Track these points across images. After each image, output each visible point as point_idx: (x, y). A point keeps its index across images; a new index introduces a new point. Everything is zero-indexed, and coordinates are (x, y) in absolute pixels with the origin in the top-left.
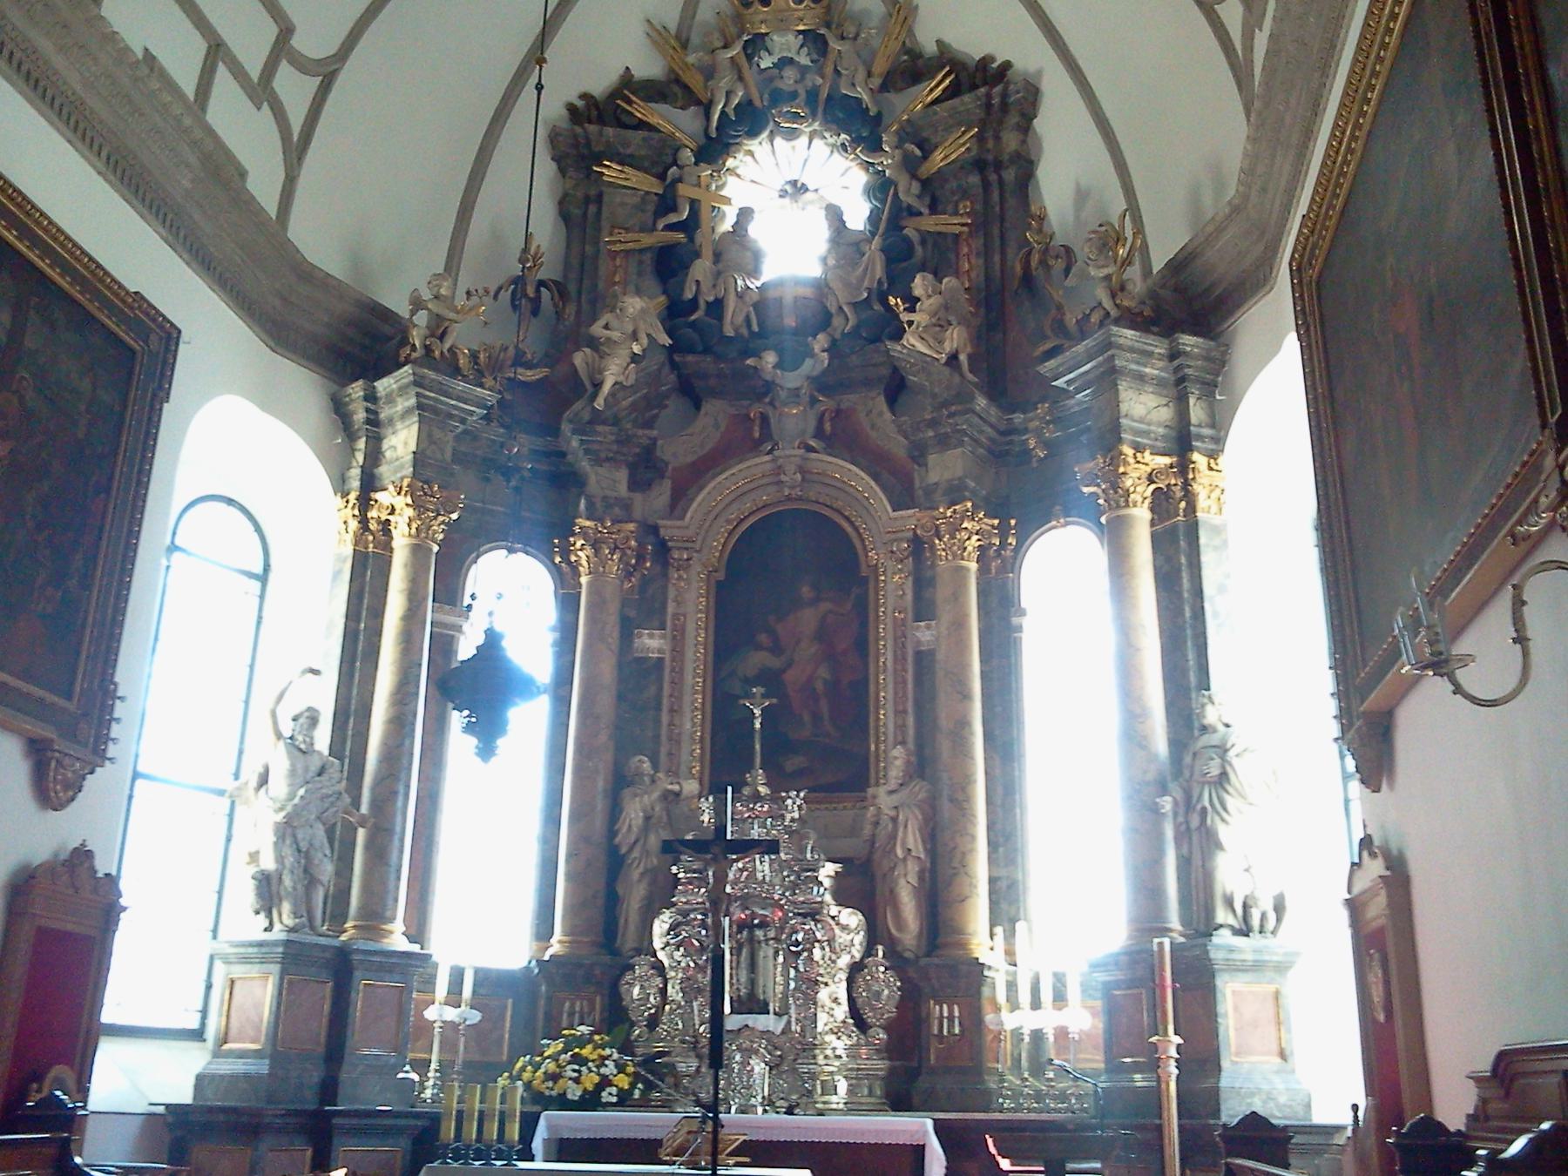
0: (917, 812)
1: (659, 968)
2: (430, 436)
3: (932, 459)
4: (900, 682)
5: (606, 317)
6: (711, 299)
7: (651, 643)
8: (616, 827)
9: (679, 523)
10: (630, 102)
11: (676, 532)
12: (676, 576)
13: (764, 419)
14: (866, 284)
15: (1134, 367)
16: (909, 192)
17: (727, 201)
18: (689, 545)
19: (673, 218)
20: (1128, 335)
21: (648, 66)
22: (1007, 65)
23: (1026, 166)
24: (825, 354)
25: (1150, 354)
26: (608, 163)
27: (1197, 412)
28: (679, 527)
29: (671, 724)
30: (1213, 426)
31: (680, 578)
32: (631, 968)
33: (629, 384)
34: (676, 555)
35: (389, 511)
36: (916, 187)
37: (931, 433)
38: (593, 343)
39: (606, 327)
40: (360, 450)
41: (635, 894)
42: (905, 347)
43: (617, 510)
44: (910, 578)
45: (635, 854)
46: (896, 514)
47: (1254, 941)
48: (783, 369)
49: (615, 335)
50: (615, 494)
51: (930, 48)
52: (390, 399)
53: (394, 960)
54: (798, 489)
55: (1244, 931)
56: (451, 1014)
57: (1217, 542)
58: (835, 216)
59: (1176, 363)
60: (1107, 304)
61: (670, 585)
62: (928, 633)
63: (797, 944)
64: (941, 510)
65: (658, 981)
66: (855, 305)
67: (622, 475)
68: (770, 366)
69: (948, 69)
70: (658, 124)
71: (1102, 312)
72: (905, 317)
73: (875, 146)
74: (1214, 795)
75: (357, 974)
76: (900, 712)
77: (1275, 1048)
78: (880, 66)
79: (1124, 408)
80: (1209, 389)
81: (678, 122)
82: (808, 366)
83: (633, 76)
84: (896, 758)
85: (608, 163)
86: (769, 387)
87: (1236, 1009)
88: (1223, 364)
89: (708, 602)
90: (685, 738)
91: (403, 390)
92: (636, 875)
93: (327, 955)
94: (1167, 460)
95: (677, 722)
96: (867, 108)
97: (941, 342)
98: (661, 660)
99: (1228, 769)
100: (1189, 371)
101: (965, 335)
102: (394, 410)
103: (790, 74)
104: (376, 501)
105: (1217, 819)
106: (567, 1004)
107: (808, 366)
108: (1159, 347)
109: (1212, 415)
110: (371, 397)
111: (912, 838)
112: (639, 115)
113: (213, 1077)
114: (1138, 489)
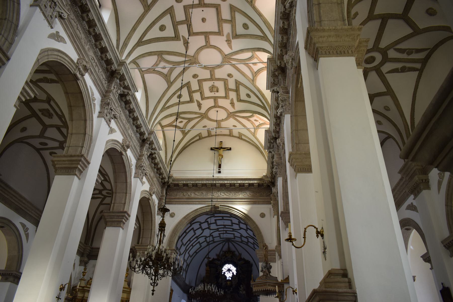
19: (217, 273)
21: (216, 257)
22: (250, 261)
51: (242, 257)
58: (233, 273)
78: (238, 259)
107: (230, 291)
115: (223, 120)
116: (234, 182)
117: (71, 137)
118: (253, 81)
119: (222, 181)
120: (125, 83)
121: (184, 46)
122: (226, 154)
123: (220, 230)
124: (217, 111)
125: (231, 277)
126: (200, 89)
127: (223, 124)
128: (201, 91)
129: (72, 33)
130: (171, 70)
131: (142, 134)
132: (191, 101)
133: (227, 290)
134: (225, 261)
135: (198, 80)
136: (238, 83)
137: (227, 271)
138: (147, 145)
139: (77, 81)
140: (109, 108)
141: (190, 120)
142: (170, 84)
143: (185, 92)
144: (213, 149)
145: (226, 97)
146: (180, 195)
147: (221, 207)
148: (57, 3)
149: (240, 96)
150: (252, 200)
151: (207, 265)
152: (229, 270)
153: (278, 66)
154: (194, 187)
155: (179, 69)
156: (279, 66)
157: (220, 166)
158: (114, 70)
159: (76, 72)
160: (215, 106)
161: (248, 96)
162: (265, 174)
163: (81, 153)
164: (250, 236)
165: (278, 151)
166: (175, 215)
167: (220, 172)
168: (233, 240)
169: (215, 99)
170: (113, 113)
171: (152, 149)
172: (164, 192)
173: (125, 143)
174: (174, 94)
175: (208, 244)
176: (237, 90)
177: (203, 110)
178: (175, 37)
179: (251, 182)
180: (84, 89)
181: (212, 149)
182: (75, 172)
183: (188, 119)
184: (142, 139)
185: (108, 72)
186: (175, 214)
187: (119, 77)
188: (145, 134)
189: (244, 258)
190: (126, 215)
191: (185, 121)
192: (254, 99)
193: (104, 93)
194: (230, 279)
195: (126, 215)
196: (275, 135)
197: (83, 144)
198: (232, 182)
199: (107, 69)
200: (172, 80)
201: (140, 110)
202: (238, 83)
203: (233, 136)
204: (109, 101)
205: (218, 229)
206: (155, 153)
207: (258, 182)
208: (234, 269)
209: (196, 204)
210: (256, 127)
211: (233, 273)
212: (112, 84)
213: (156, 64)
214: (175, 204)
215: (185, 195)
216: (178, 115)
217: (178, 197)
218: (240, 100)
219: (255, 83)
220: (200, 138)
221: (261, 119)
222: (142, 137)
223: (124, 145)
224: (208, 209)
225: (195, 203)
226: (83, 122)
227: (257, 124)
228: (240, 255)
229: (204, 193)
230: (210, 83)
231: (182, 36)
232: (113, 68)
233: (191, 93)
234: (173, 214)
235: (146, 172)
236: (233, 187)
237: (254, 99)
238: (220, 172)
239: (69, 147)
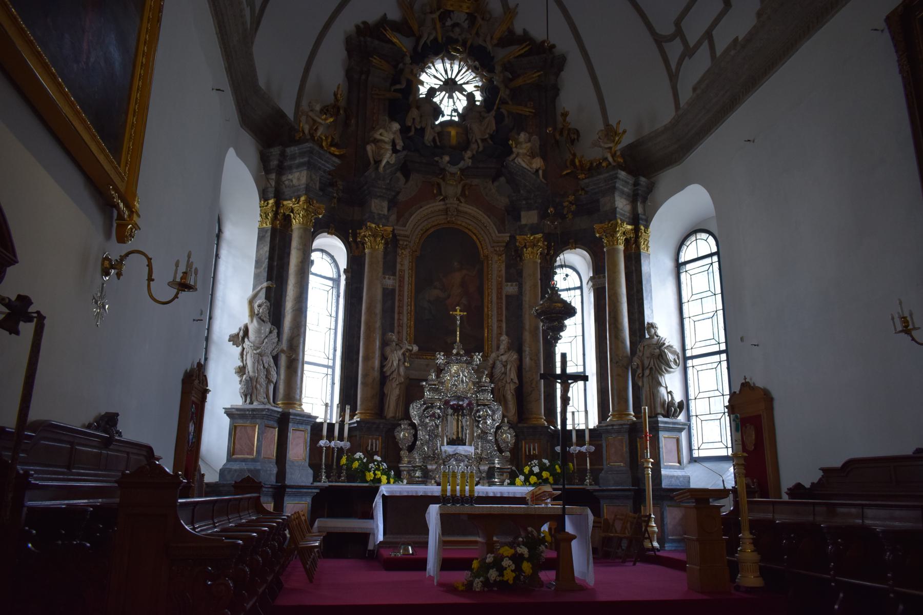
0: (514, 363)
1: (413, 426)
2: (311, 177)
3: (523, 214)
4: (499, 308)
5: (381, 131)
6: (419, 127)
7: (511, 289)
8: (385, 363)
9: (404, 228)
10: (386, 30)
11: (402, 233)
12: (400, 252)
13: (439, 185)
14: (488, 131)
15: (621, 187)
16: (504, 93)
17: (422, 83)
18: (406, 239)
19: (398, 87)
20: (622, 174)
21: (394, 14)
22: (553, 46)
23: (556, 90)
24: (470, 160)
25: (627, 183)
26: (375, 56)
27: (640, 210)
28: (403, 230)
29: (399, 319)
30: (644, 214)
31: (402, 253)
32: (400, 425)
33: (392, 163)
34: (401, 242)
35: (290, 211)
36: (508, 92)
37: (524, 202)
38: (376, 141)
39: (381, 135)
40: (272, 179)
41: (394, 393)
42: (516, 163)
43: (384, 220)
44: (504, 263)
45: (395, 375)
46: (500, 235)
48: (451, 164)
49: (386, 139)
50: (383, 213)
52: (293, 157)
53: (305, 419)
54: (454, 219)
55: (667, 415)
56: (341, 444)
57: (647, 262)
58: (470, 97)
59: (636, 188)
60: (610, 159)
61: (398, 256)
62: (512, 288)
63: (479, 417)
64: (528, 236)
65: (412, 431)
66: (483, 140)
67: (385, 204)
68: (446, 162)
69: (528, 43)
70: (396, 42)
71: (607, 162)
72: (514, 150)
73: (491, 70)
74: (655, 361)
75: (290, 425)
76: (499, 321)
77: (677, 460)
79: (617, 203)
80: (644, 201)
81: (403, 43)
82: (462, 165)
83: (387, 18)
84: (503, 340)
85: (375, 56)
86: (443, 170)
87: (665, 445)
88: (651, 191)
89: (412, 265)
90: (405, 326)
91: (302, 154)
92: (394, 385)
93: (279, 416)
94: (629, 227)
95: (401, 318)
96: (489, 52)
97: (531, 164)
99: (663, 354)
100: (640, 192)
101: (542, 162)
102: (292, 162)
103: (457, 30)
104: (283, 205)
105: (657, 372)
106: (370, 441)
107: (462, 165)
108: (631, 180)
109: (644, 210)
110: (283, 155)
111: (513, 375)
112: (388, 36)
113: (230, 470)
114: (621, 238)
125: (459, 115)
133: (447, 158)
134: (436, 39)
137: (441, 89)
152: (450, 86)
189: (525, 32)
194: (456, 119)
208: (471, 82)
211: (470, 97)
228: (510, 12)
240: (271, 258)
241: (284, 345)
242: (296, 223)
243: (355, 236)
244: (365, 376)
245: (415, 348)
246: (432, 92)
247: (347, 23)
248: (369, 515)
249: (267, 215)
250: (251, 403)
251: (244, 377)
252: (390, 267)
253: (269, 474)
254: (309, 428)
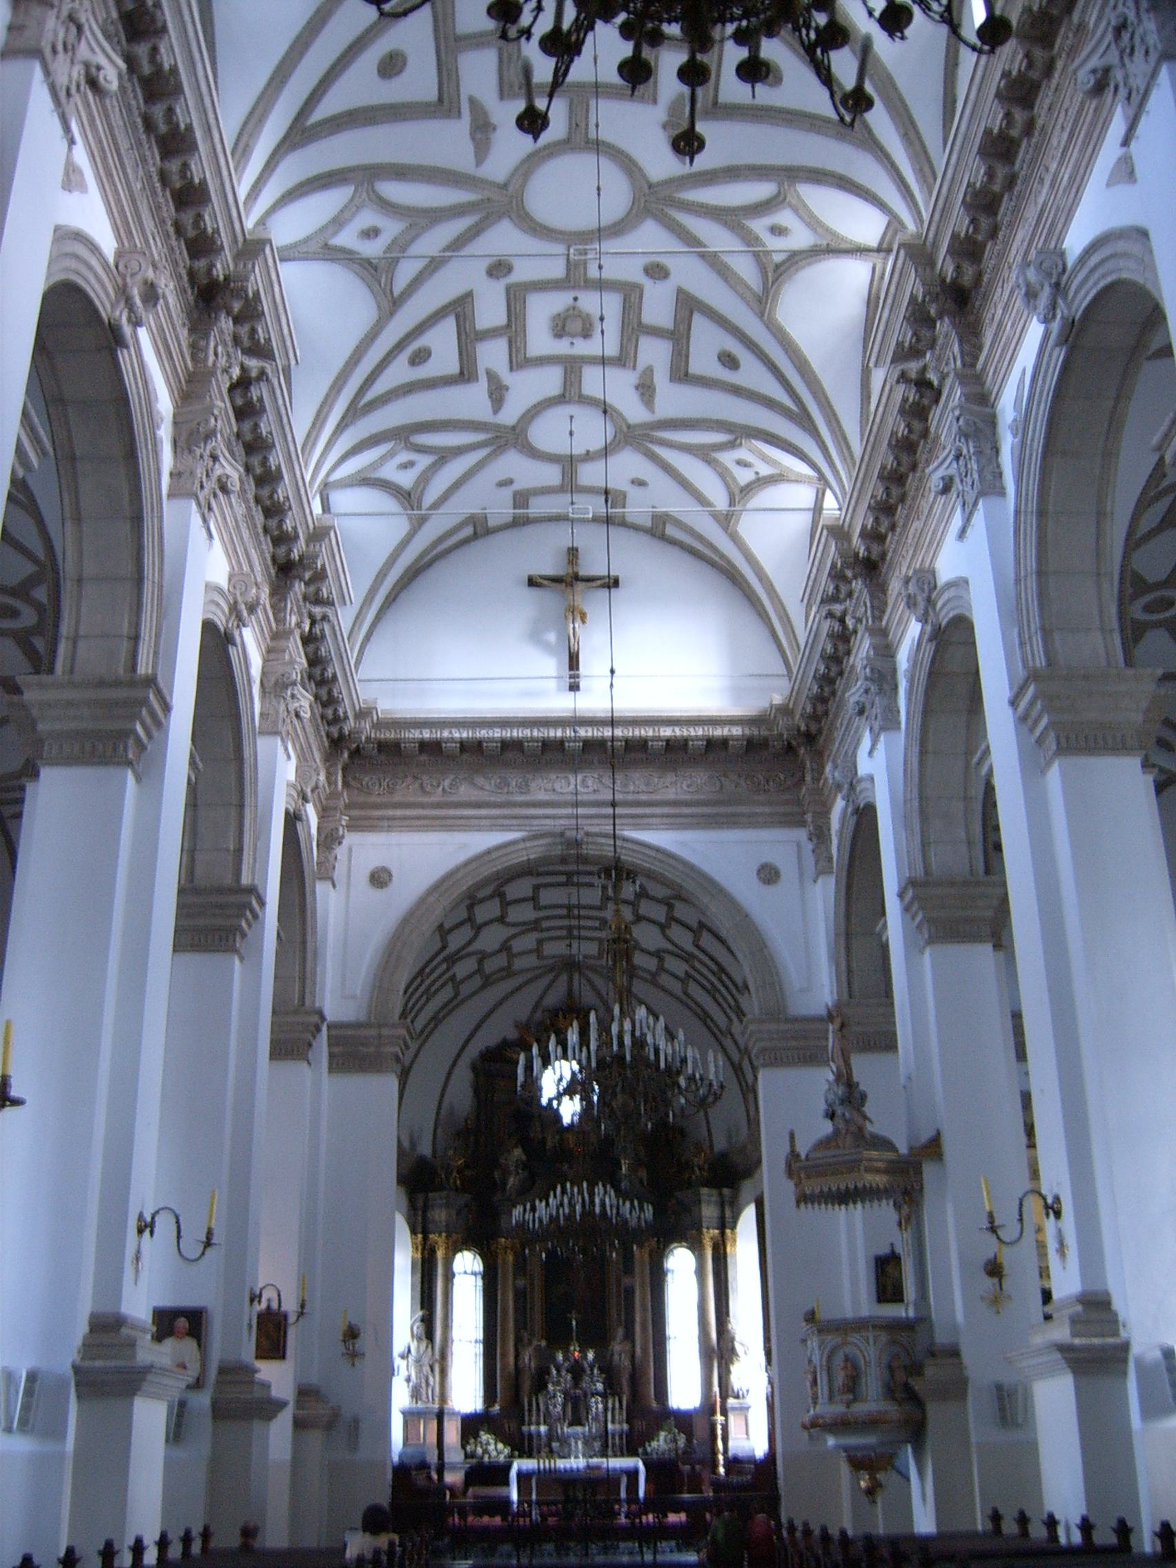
21: (512, 1034)
27: (728, 1213)
41: (527, 1385)
47: (741, 1401)
79: (703, 1213)
94: (717, 1231)
98: (525, 1288)
108: (714, 1192)
115: (588, 457)
116: (643, 732)
117: (80, 592)
118: (763, 302)
119: (590, 729)
120: (260, 331)
121: (473, 139)
122: (594, 602)
123: (545, 924)
124: (572, 417)
126: (509, 326)
127: (590, 474)
128: (514, 329)
129: (100, 142)
130: (399, 247)
131: (281, 539)
132: (465, 375)
135: (508, 289)
136: (688, 305)
138: (299, 588)
139: (116, 350)
140: (208, 452)
141: (444, 456)
142: (392, 304)
143: (443, 340)
144: (539, 580)
145: (623, 359)
146: (406, 790)
147: (590, 839)
148: (86, 28)
149: (687, 356)
150: (722, 810)
151: (474, 1068)
153: (944, 281)
154: (465, 756)
155: (434, 241)
156: (948, 280)
157: (573, 661)
158: (221, 278)
159: (118, 313)
160: (563, 396)
161: (729, 361)
162: (778, 699)
163: (134, 668)
164: (675, 949)
165: (878, 617)
166: (390, 875)
167: (574, 687)
168: (592, 962)
169: (572, 367)
170: (218, 471)
171: (318, 601)
172: (336, 779)
173: (241, 594)
174: (399, 346)
175: (487, 982)
176: (679, 337)
177: (510, 415)
178: (440, 100)
179: (718, 732)
180: (136, 383)
181: (532, 582)
182: (126, 750)
183: (435, 453)
184: (282, 560)
185: (193, 288)
186: (394, 873)
187: (237, 306)
188: (297, 537)
190: (254, 902)
191: (424, 461)
192: (752, 375)
193: (183, 382)
195: (254, 902)
196: (868, 549)
197: (137, 625)
198: (637, 733)
199: (192, 274)
200: (397, 292)
201: (290, 439)
202: (688, 305)
203: (623, 524)
204: (213, 420)
205: (537, 921)
206: (325, 618)
207: (747, 732)
209: (479, 829)
210: (737, 492)
212: (207, 337)
213: (338, 222)
214: (389, 829)
215: (429, 788)
216: (402, 435)
217: (397, 798)
218: (686, 374)
219: (773, 309)
220: (475, 533)
221: (765, 459)
222: (282, 551)
223: (240, 599)
224: (534, 851)
225: (476, 822)
226: (126, 528)
227: (744, 477)
229: (514, 779)
230: (558, 302)
231: (472, 101)
232: (219, 272)
233: (468, 339)
234: (385, 876)
235: (297, 705)
236: (640, 756)
237: (752, 375)
238: (574, 687)
239: (75, 641)
240: (422, 1283)
241: (437, 1356)
242: (440, 1254)
243: (489, 1248)
244: (503, 1370)
245: (544, 1343)
246: (550, 1100)
247: (474, 1051)
248: (506, 1483)
249: (417, 1249)
250: (417, 1402)
251: (411, 1384)
252: (521, 1266)
253: (432, 1458)
254: (459, 1418)
